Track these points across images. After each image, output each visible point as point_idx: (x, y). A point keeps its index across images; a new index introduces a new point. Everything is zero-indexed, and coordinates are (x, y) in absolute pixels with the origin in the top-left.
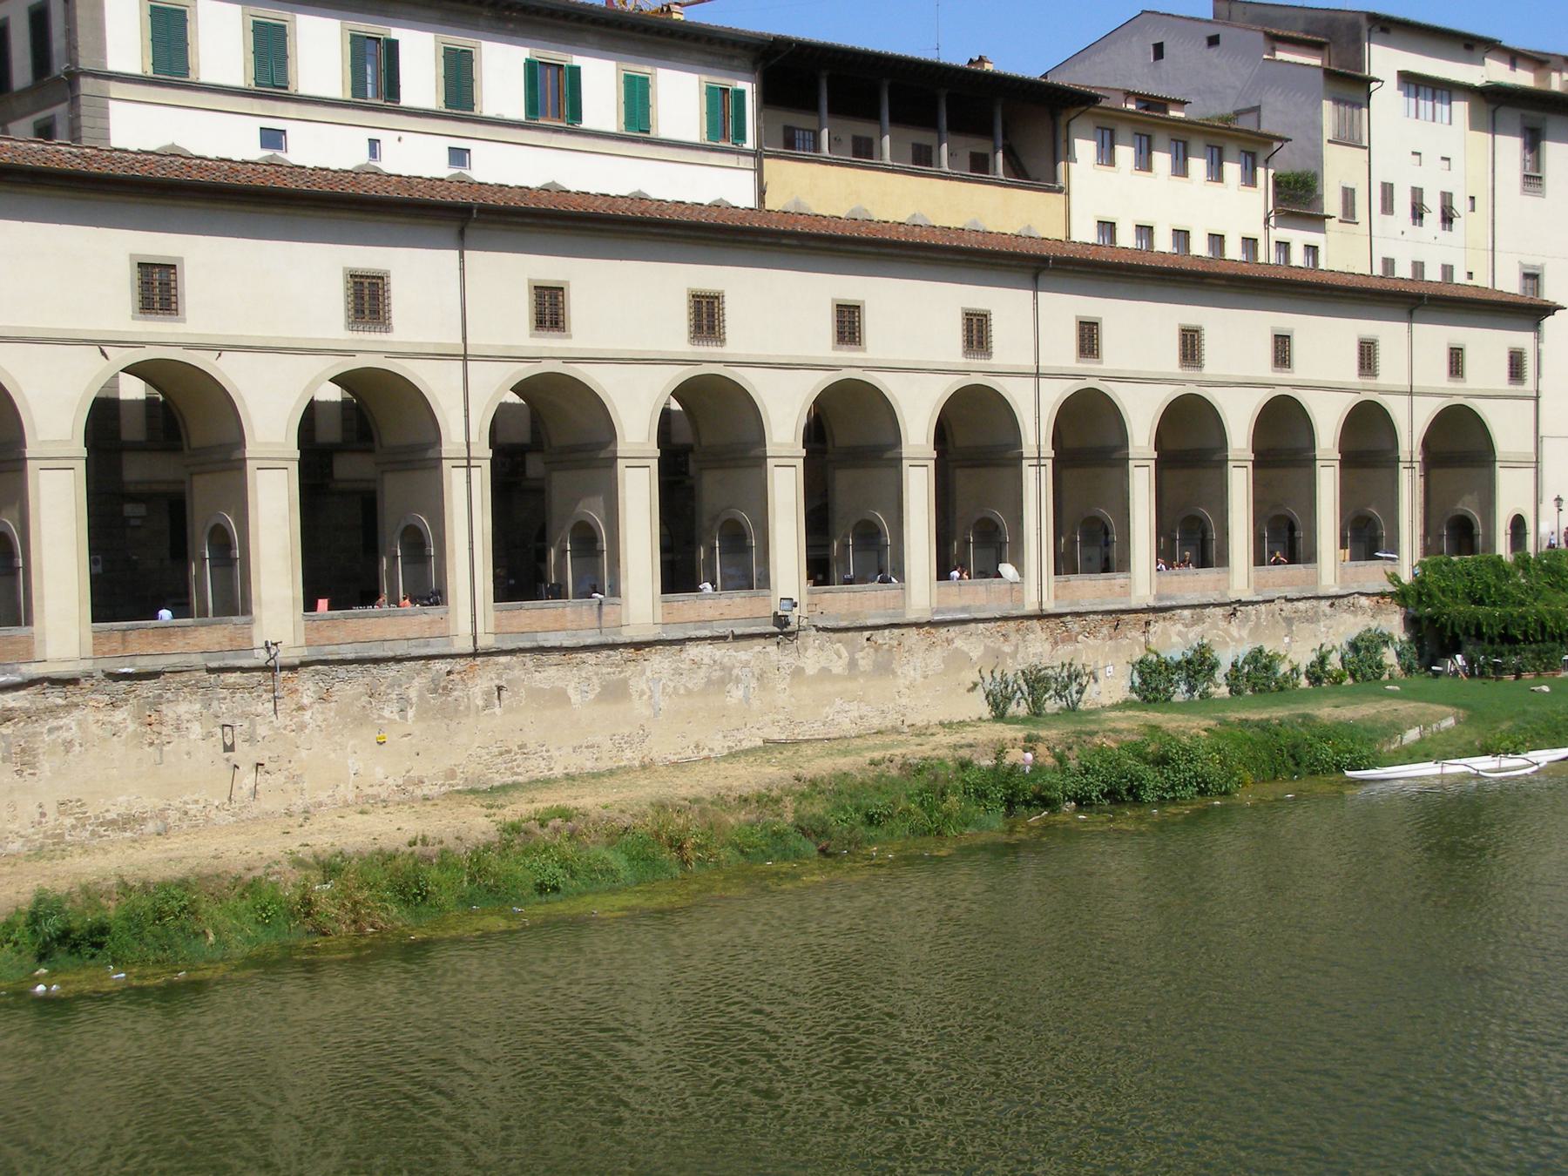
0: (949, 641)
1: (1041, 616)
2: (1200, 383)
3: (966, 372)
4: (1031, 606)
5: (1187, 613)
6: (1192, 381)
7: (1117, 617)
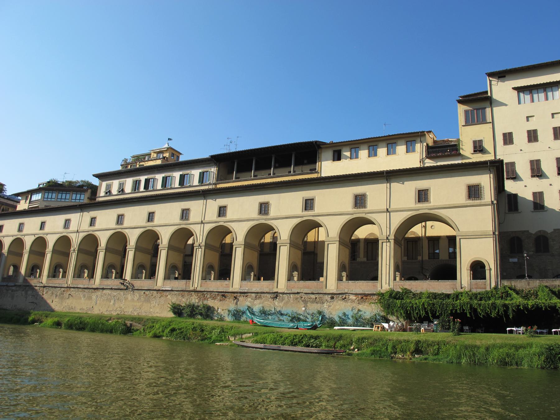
0: (167, 296)
1: (195, 291)
2: (266, 220)
3: (180, 225)
4: (191, 288)
5: (253, 295)
6: (263, 219)
7: (224, 295)
